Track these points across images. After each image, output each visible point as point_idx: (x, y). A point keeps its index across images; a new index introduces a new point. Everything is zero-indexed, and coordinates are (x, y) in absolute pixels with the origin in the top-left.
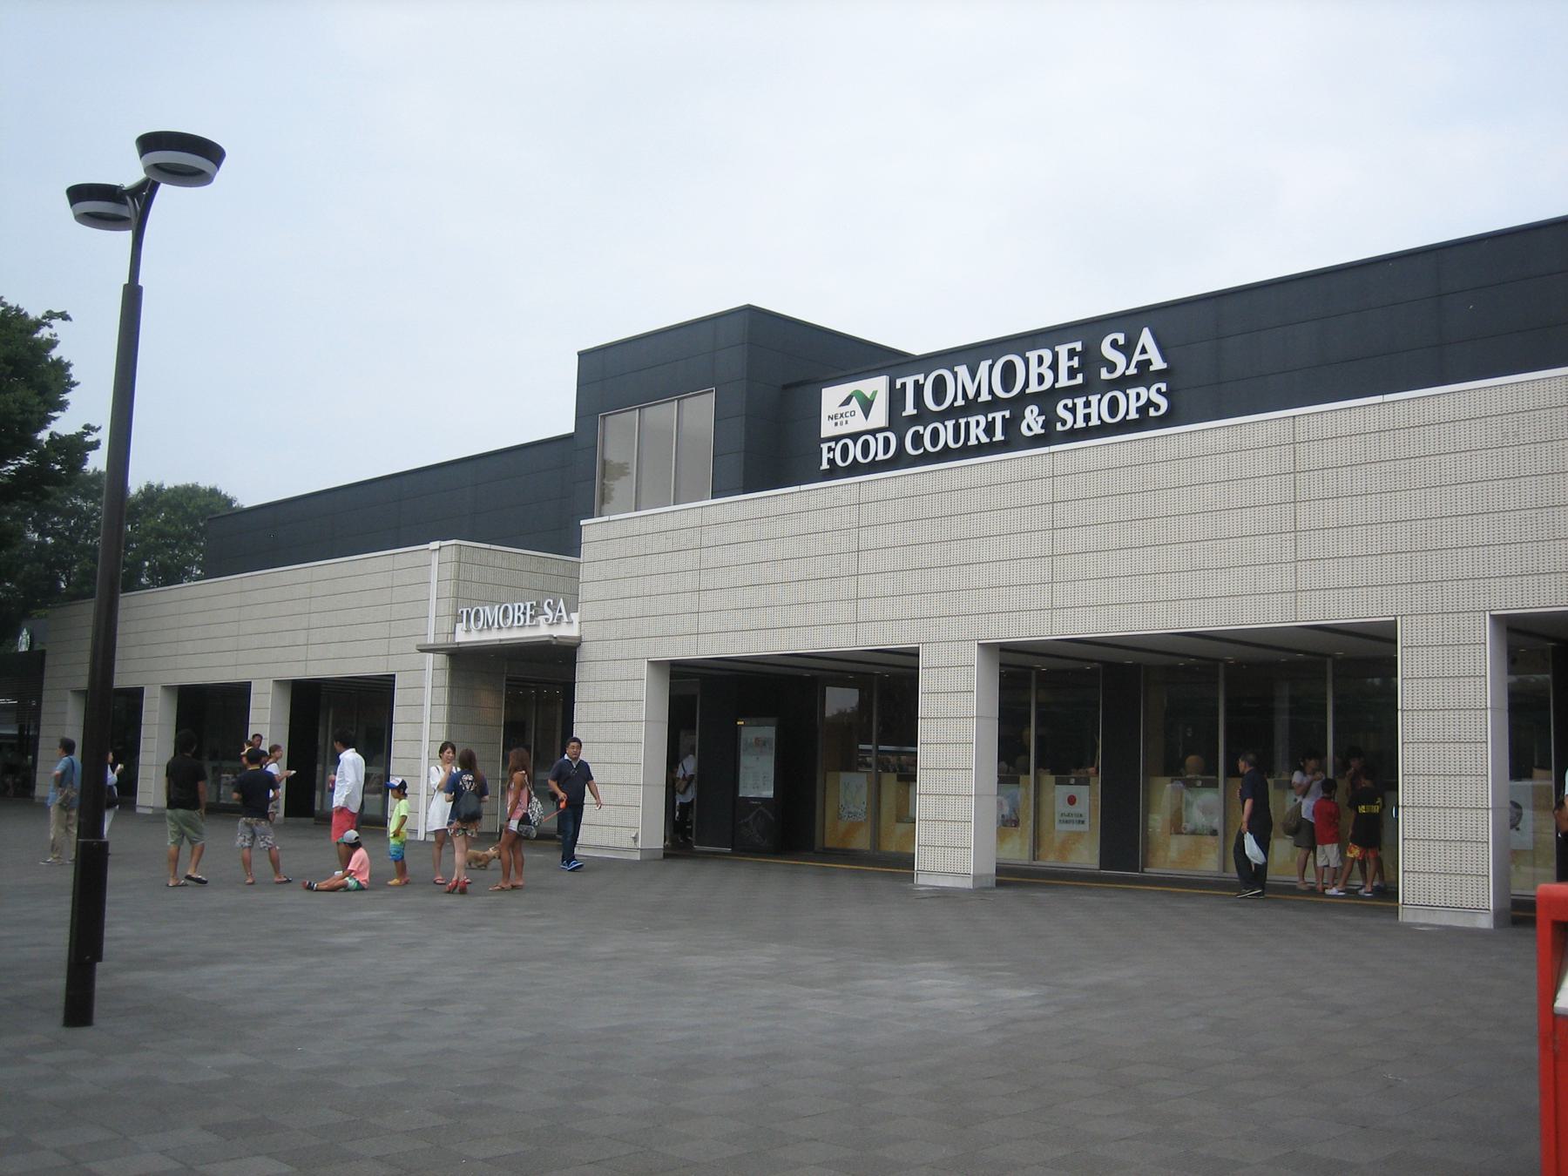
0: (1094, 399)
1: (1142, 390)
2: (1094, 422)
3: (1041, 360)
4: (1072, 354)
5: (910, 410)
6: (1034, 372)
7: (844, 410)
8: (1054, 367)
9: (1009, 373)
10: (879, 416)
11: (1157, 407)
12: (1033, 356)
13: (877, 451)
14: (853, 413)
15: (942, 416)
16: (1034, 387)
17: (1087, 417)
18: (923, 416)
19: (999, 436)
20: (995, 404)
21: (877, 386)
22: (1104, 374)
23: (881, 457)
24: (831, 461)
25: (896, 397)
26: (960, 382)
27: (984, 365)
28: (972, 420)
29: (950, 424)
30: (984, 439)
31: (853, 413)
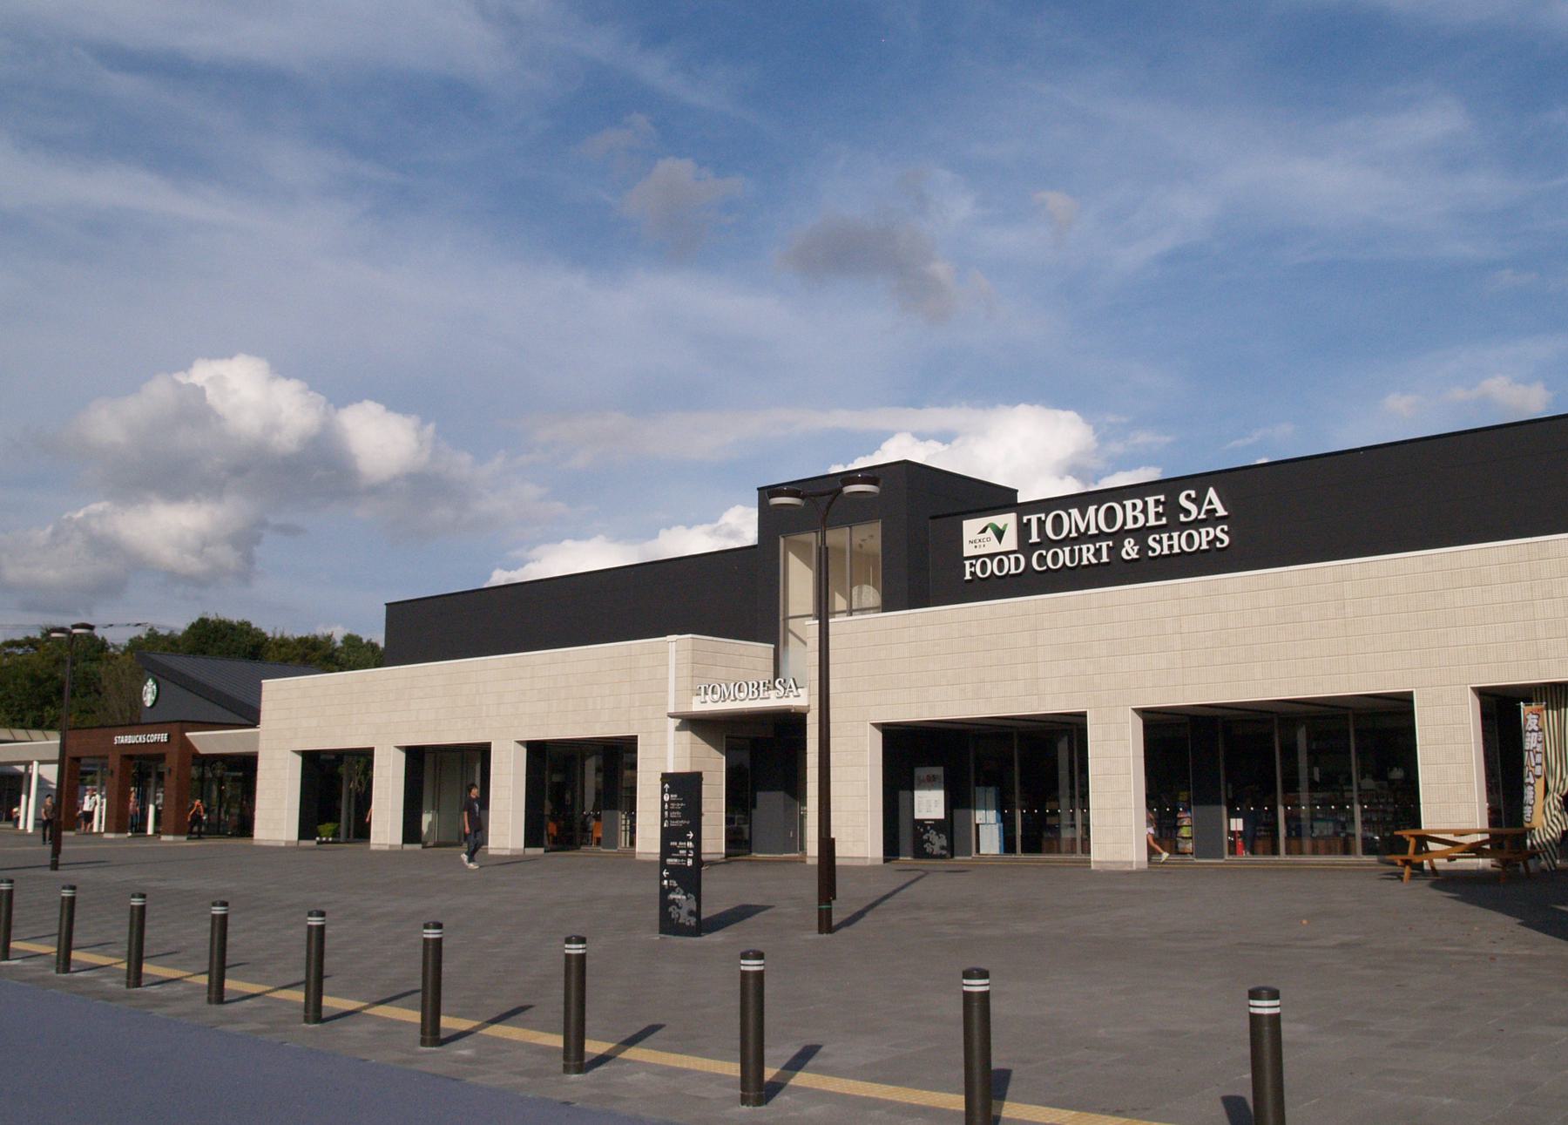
0: (1175, 535)
1: (1211, 530)
2: (1176, 550)
3: (1134, 506)
4: (1157, 503)
5: (1035, 539)
6: (1130, 514)
7: (979, 537)
8: (1145, 511)
9: (1111, 514)
10: (1010, 541)
11: (1222, 541)
12: (1128, 503)
13: (1010, 567)
14: (989, 539)
15: (1060, 544)
16: (1130, 525)
17: (1171, 547)
18: (1046, 543)
19: (1105, 559)
20: (1101, 536)
21: (1008, 520)
22: (1182, 518)
23: (1013, 571)
24: (973, 574)
25: (1024, 529)
26: (1073, 520)
27: (1092, 509)
28: (1084, 547)
29: (1067, 550)
30: (1094, 561)
31: (989, 539)
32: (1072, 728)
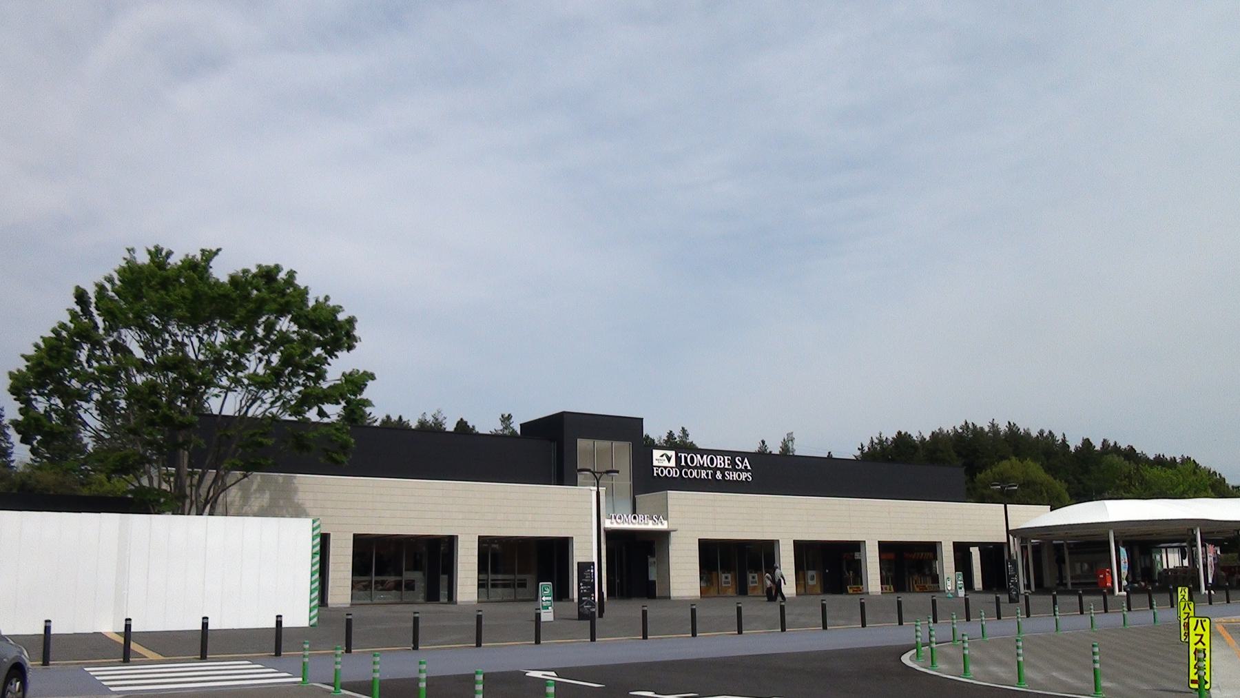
6: (719, 461)
10: (673, 463)
13: (673, 473)
18: (688, 467)
20: (709, 468)
25: (678, 459)
32: (451, 541)
